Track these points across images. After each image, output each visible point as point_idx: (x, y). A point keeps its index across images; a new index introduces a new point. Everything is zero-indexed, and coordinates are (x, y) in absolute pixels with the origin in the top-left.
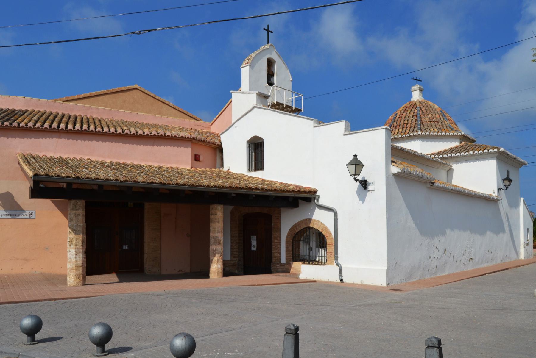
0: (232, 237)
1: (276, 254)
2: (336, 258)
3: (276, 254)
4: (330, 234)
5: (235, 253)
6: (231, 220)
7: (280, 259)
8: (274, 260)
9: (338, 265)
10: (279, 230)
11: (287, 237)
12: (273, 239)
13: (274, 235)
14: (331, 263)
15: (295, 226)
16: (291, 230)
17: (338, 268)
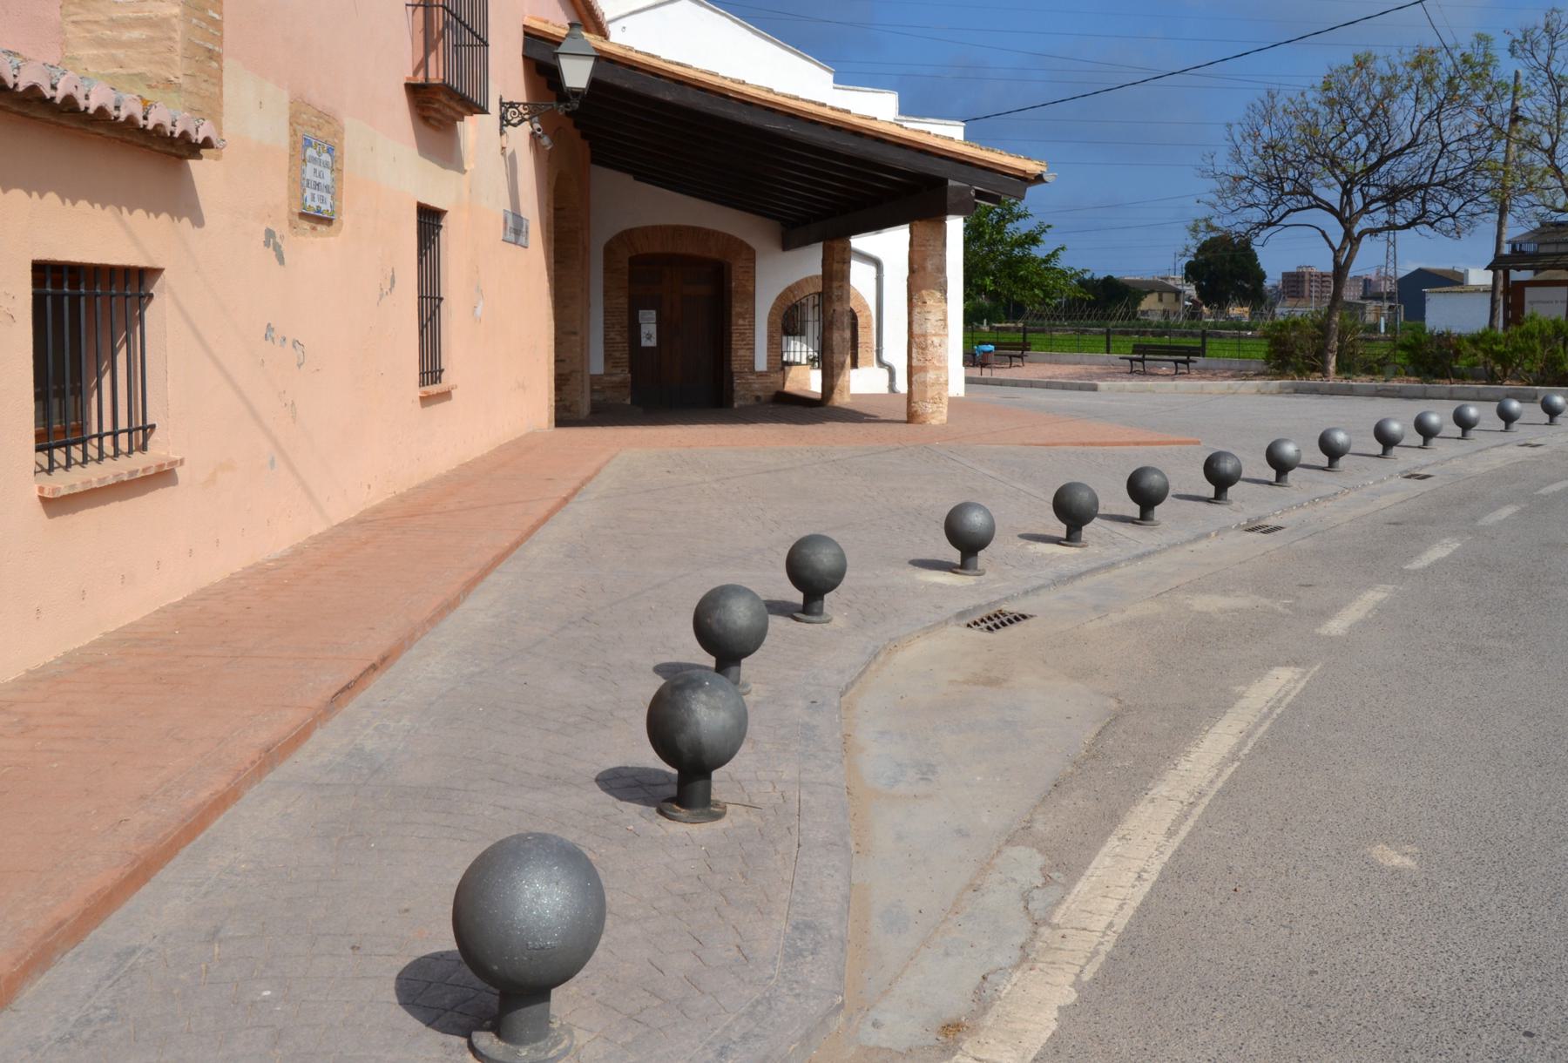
0: (606, 311)
1: (741, 352)
2: (879, 353)
3: (741, 352)
4: (866, 307)
5: (617, 354)
6: (606, 269)
7: (753, 362)
8: (735, 366)
9: (881, 363)
10: (751, 297)
11: (771, 314)
12: (734, 319)
13: (737, 308)
14: (869, 363)
15: (790, 289)
16: (781, 298)
17: (884, 373)
